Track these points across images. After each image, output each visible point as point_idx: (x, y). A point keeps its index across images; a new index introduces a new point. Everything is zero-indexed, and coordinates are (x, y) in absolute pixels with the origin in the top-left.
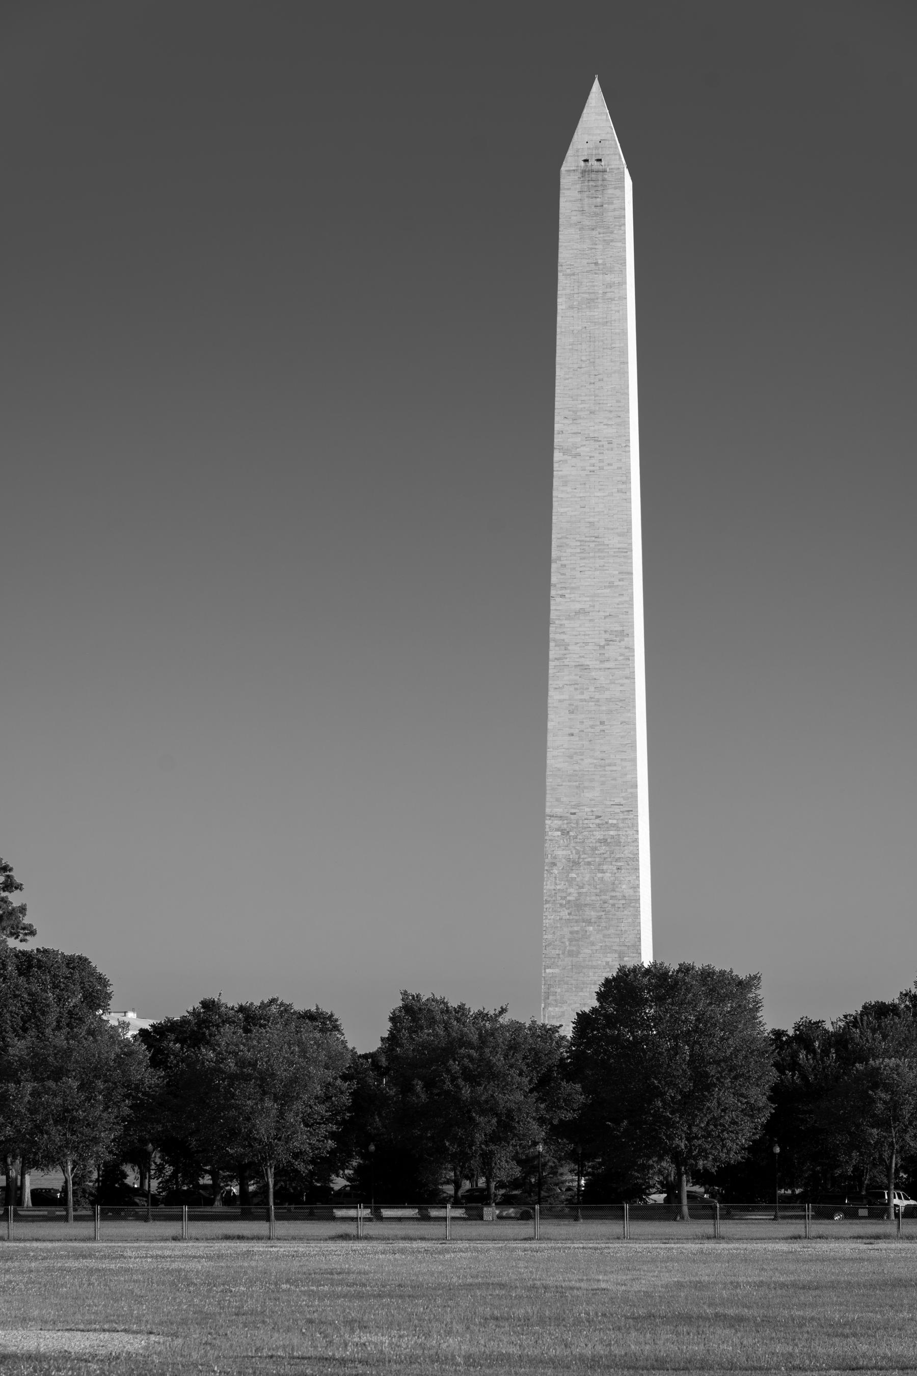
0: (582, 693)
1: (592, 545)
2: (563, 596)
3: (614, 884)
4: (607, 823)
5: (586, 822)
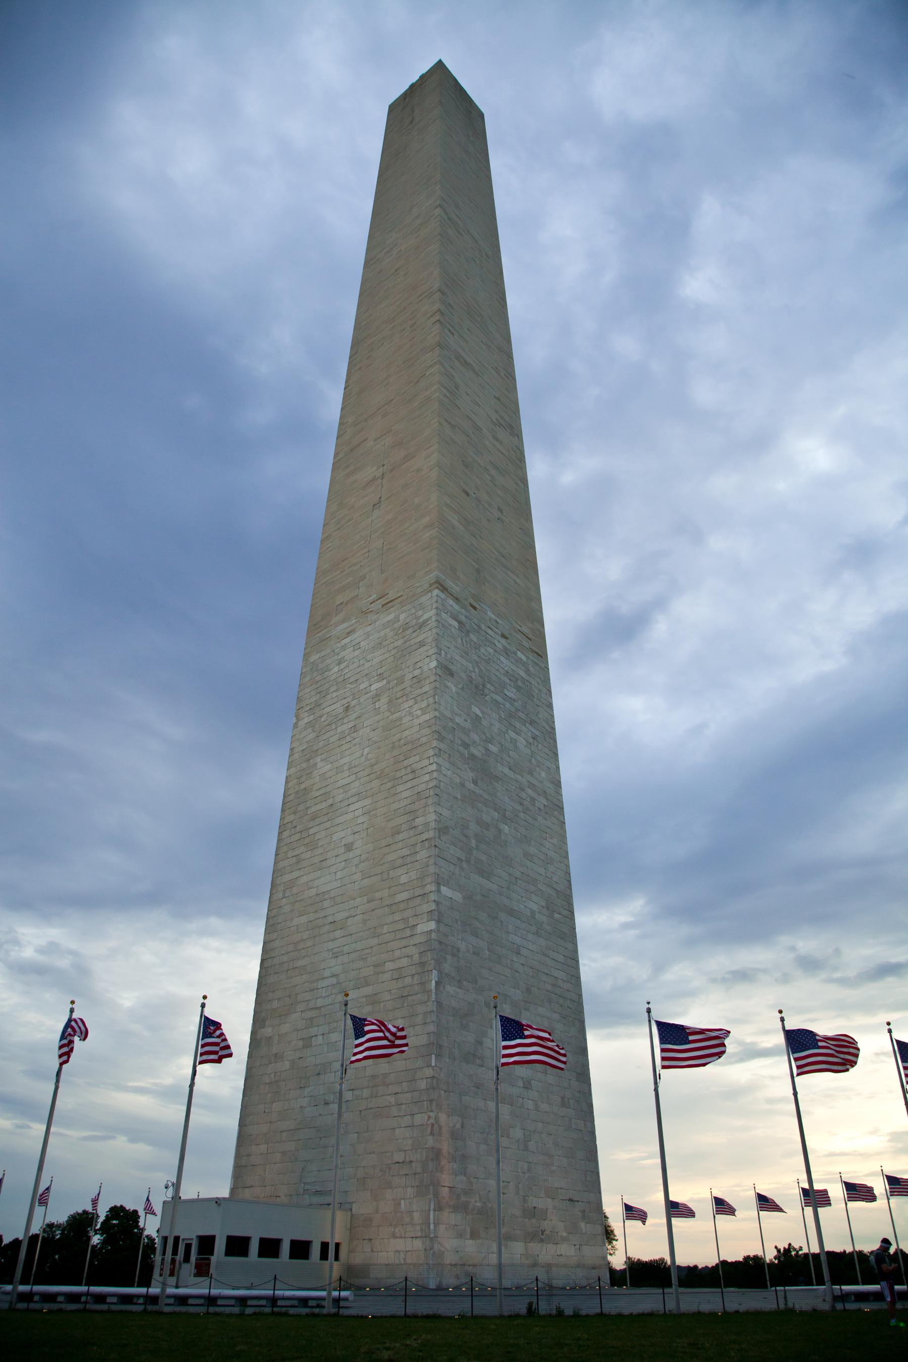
3: (530, 761)
4: (516, 654)
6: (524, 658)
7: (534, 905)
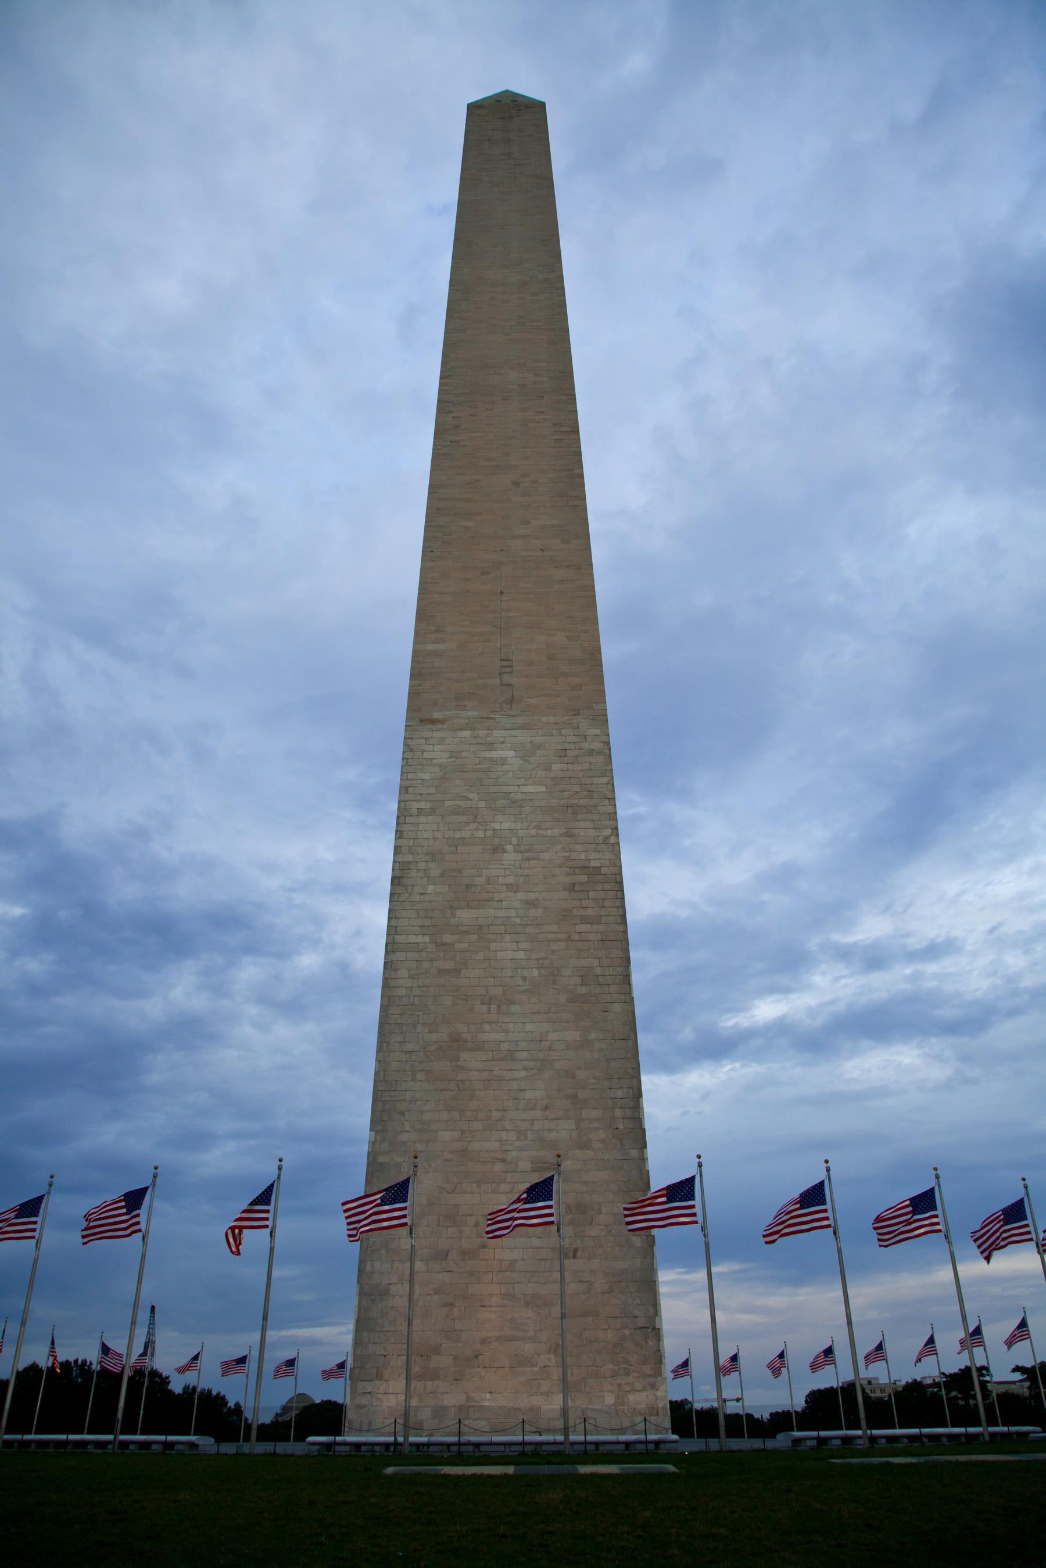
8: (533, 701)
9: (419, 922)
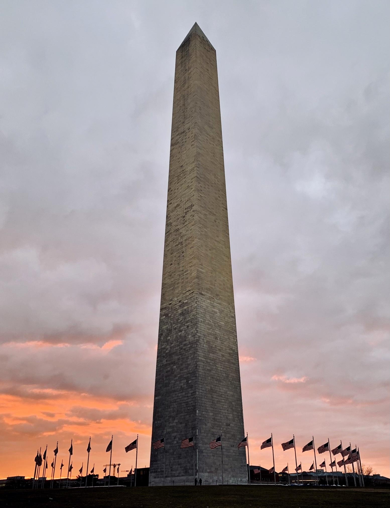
0: (176, 242)
1: (181, 175)
2: (171, 203)
3: (185, 337)
4: (183, 303)
5: (175, 306)
6: (187, 301)
7: (183, 383)
8: (221, 297)
9: (202, 354)
